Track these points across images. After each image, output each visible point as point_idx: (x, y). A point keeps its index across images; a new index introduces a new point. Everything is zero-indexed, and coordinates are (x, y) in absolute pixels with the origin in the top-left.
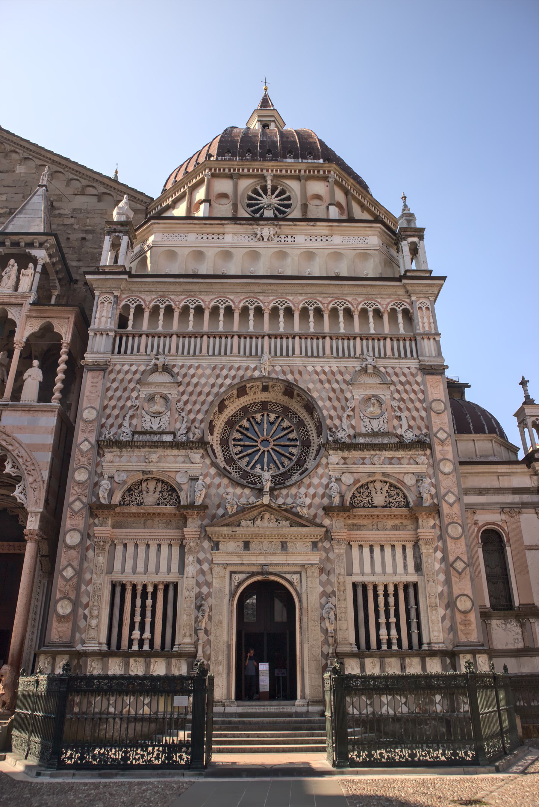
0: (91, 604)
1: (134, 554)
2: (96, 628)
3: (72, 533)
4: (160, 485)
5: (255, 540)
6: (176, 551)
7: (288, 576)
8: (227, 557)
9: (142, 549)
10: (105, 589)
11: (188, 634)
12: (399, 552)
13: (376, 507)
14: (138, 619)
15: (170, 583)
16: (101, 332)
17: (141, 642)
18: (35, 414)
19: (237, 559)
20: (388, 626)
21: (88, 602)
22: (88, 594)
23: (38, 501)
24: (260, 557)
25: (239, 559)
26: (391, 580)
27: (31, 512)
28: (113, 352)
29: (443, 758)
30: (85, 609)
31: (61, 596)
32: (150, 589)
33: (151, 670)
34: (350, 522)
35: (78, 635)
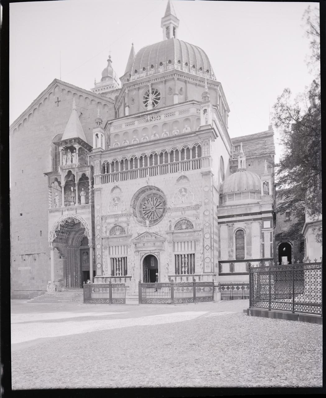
3: (98, 245)
4: (120, 228)
6: (126, 247)
7: (155, 253)
9: (117, 248)
12: (190, 244)
13: (183, 229)
14: (118, 267)
16: (97, 176)
17: (119, 274)
20: (185, 267)
26: (186, 253)
28: (102, 183)
29: (163, 303)
32: (120, 259)
34: (174, 235)
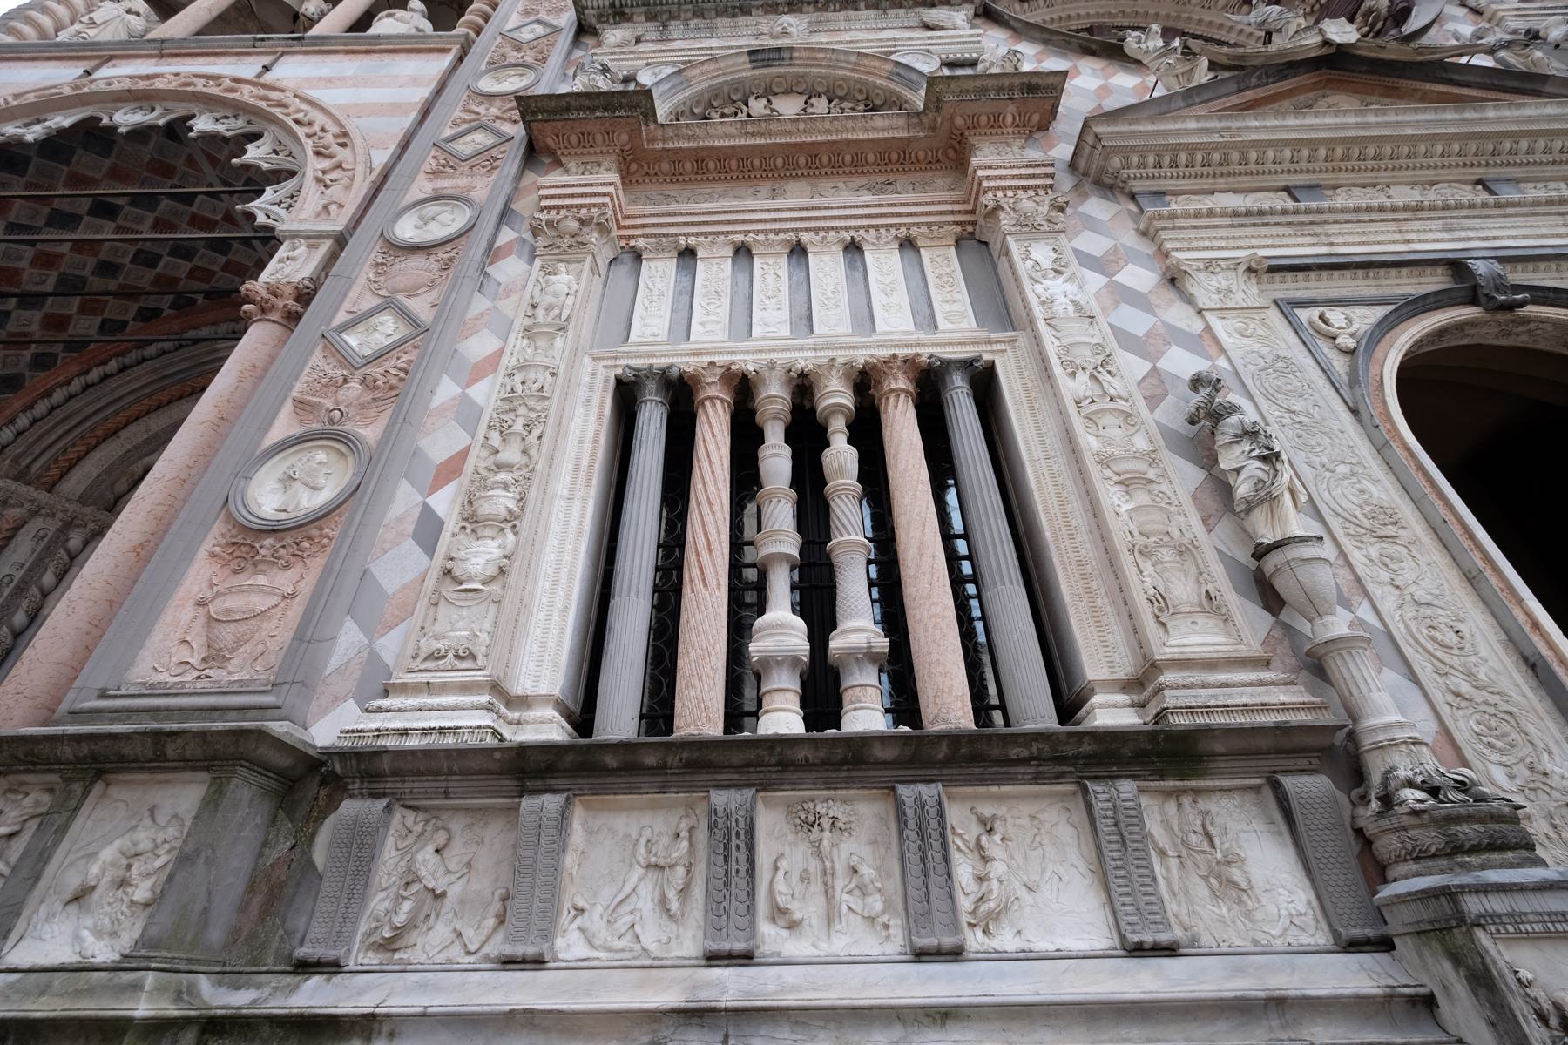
0: (477, 460)
1: (734, 284)
2: (495, 588)
5: (1343, 177)
8: (1238, 232)
10: (581, 410)
11: (1183, 590)
15: (947, 365)
18: (386, 58)
19: (1300, 240)
21: (463, 455)
22: (467, 414)
23: (333, 208)
24: (1416, 225)
25: (1308, 240)
27: (294, 235)
30: (435, 488)
31: (297, 430)
32: (836, 396)
33: (965, 904)
35: (348, 640)
